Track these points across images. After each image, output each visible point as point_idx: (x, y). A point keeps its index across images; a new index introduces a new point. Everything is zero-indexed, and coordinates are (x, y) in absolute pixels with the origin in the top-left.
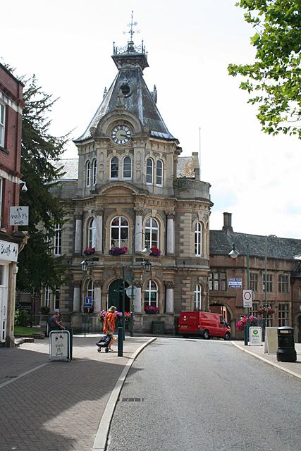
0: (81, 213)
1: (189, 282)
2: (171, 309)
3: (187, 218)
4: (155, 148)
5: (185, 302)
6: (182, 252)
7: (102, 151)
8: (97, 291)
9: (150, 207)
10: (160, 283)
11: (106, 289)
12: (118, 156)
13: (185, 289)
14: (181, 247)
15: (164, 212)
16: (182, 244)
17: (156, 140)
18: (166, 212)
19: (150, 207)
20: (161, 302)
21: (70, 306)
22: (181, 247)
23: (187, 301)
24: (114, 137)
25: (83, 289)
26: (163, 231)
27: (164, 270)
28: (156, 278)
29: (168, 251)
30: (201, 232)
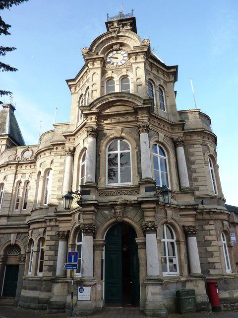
0: (72, 149)
1: (212, 227)
2: (197, 269)
3: (197, 150)
4: (156, 73)
5: (212, 257)
6: (198, 189)
7: (95, 71)
8: (87, 242)
9: (155, 128)
10: (179, 229)
11: (101, 238)
12: (114, 75)
13: (208, 238)
14: (196, 184)
15: (172, 139)
16: (196, 179)
17: (155, 63)
18: (175, 139)
19: (155, 128)
20: (183, 257)
21: (53, 269)
22: (196, 184)
23: (215, 254)
24: (108, 61)
25: (71, 242)
26: (173, 161)
27: (182, 210)
28: (172, 221)
29: (181, 185)
30: (213, 169)
